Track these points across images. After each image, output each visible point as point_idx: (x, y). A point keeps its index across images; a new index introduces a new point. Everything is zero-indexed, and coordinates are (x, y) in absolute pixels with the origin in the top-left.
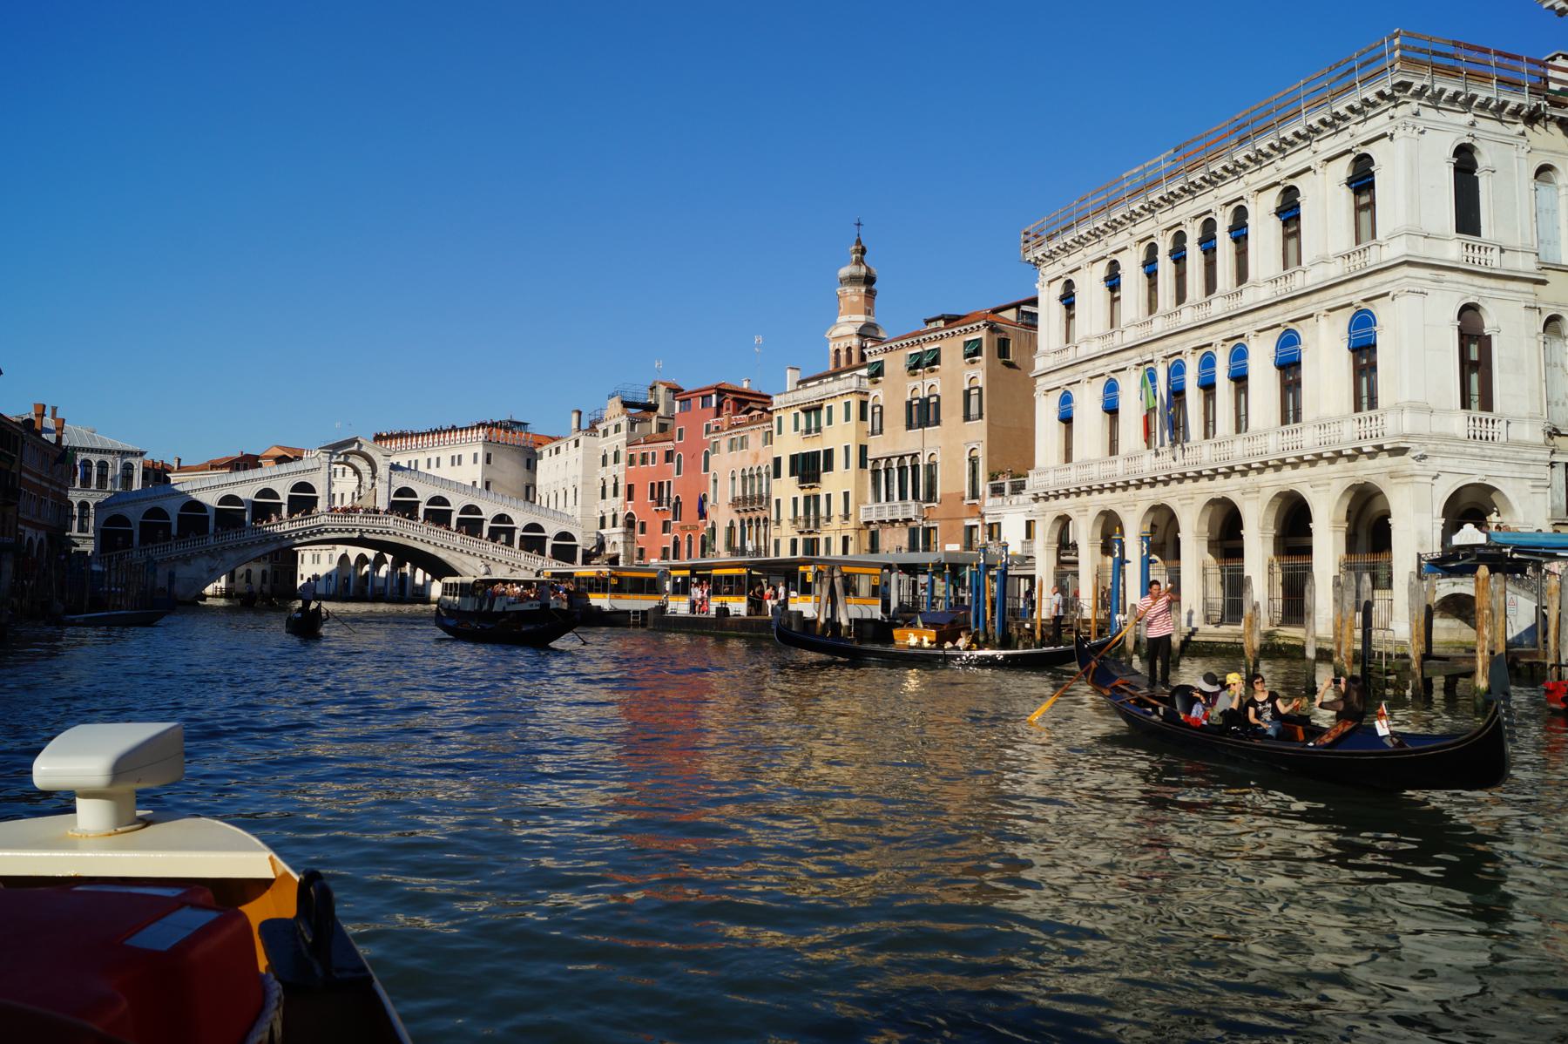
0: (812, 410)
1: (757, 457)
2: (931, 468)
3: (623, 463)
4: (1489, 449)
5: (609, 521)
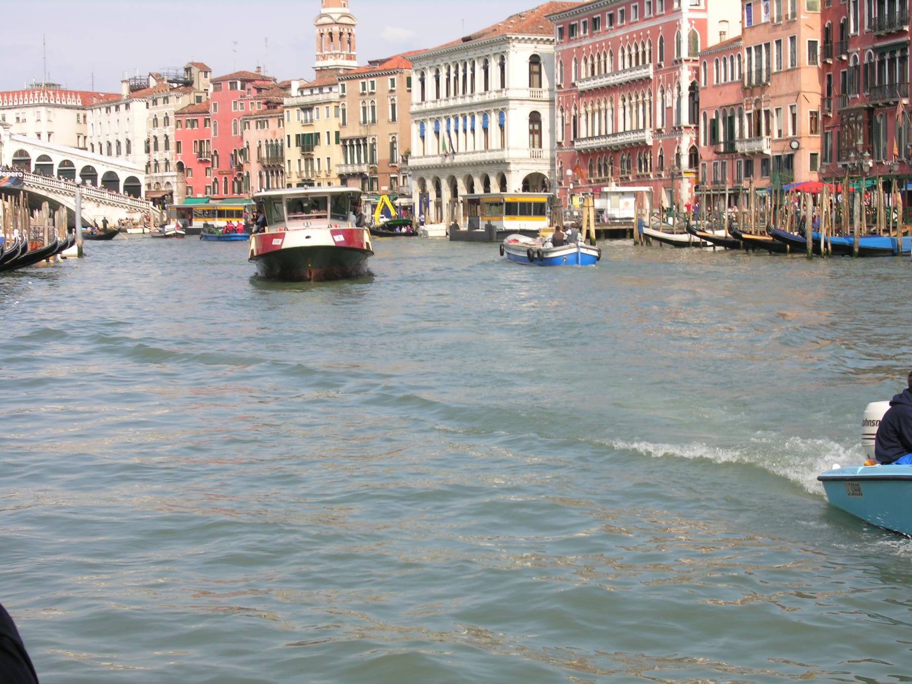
0: (307, 108)
1: (274, 133)
2: (372, 145)
3: (172, 126)
4: (539, 161)
5: (162, 167)
